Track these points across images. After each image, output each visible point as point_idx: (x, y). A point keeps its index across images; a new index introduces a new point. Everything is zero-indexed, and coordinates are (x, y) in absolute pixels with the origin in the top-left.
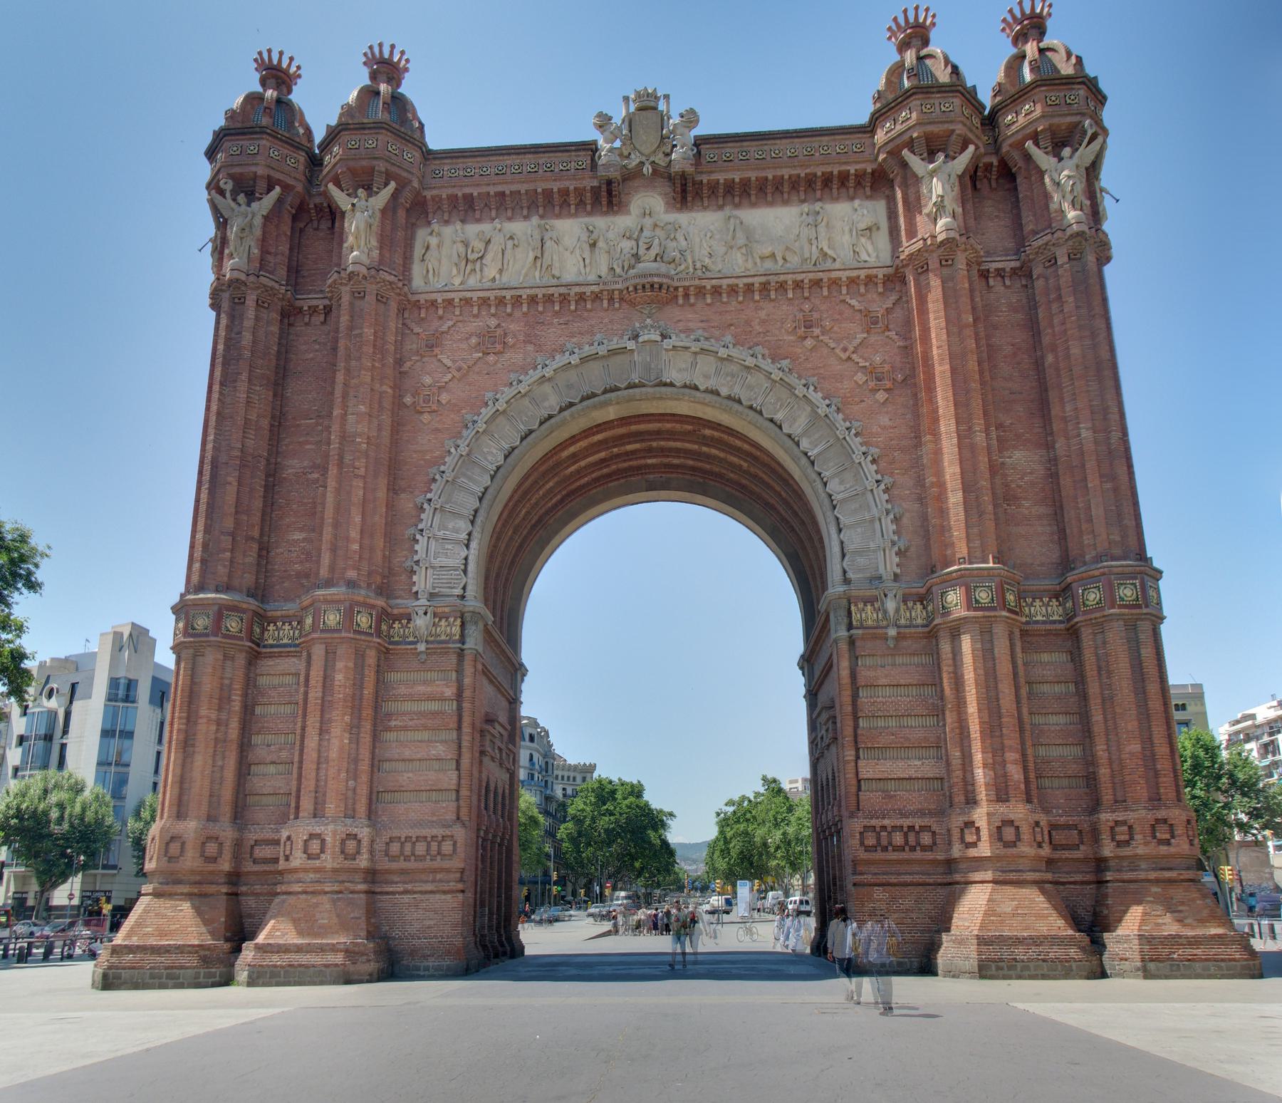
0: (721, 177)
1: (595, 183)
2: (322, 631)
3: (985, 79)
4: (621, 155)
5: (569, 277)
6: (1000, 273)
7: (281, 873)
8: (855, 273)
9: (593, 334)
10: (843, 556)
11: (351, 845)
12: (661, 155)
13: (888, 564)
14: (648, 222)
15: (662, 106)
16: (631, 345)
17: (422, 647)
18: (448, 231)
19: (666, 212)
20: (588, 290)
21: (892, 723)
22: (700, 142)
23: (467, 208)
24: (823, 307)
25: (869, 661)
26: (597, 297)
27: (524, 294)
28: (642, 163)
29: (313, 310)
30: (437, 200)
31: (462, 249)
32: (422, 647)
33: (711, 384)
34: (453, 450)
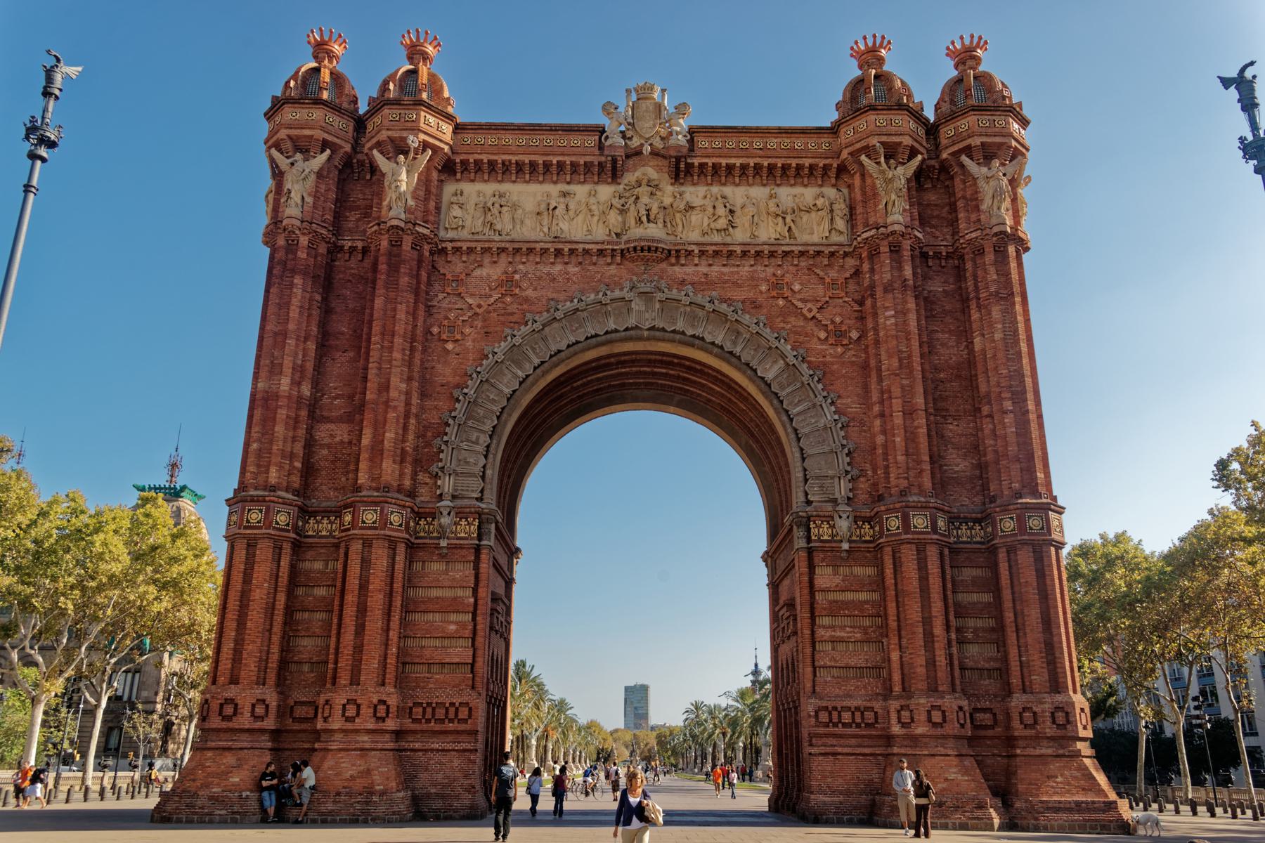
0: (710, 161)
1: (603, 159)
2: (362, 528)
3: (928, 98)
4: (624, 137)
6: (937, 255)
7: (317, 735)
10: (806, 481)
11: (382, 708)
12: (658, 139)
13: (842, 489)
16: (628, 296)
17: (443, 543)
22: (692, 131)
26: (601, 252)
28: (642, 145)
30: (464, 163)
33: (698, 332)
34: (475, 375)
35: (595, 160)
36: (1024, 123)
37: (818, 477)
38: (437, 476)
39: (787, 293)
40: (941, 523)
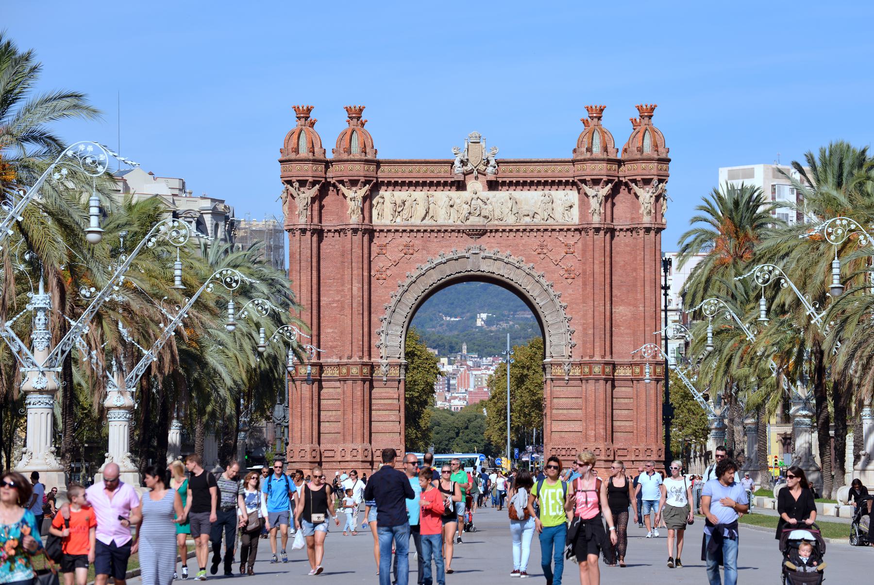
0: (508, 180)
5: (441, 221)
6: (621, 230)
8: (562, 227)
9: (451, 247)
13: (566, 351)
14: (475, 196)
16: (467, 255)
19: (483, 190)
20: (449, 229)
21: (565, 412)
22: (498, 163)
23: (395, 184)
24: (549, 240)
25: (558, 389)
26: (453, 231)
27: (422, 229)
29: (329, 231)
30: (383, 182)
33: (501, 273)
35: (449, 180)
37: (555, 345)
39: (545, 251)
40: (607, 370)
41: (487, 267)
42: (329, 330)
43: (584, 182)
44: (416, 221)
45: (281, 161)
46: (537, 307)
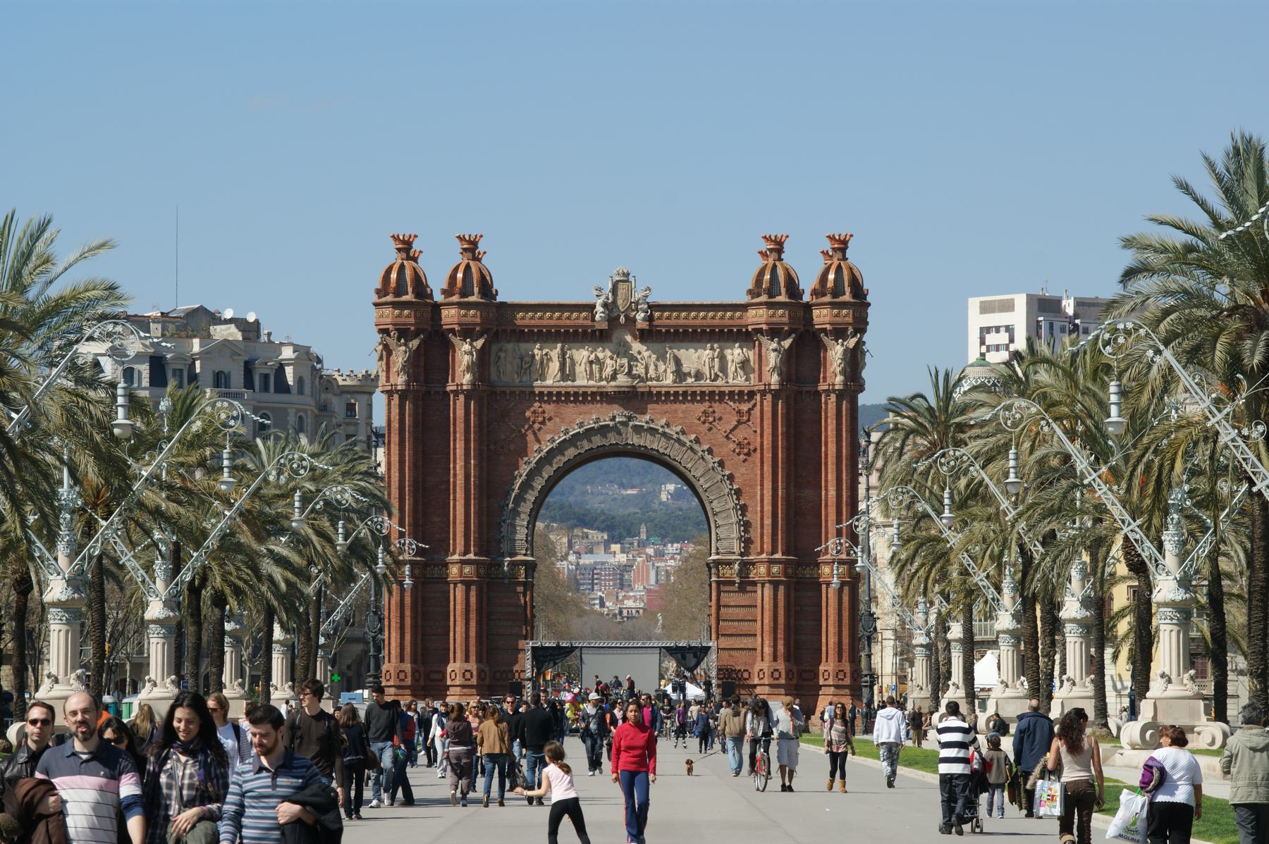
15: (631, 279)
16: (611, 423)
17: (506, 581)
18: (510, 346)
20: (589, 391)
22: (651, 307)
26: (593, 394)
30: (505, 331)
31: (518, 361)
32: (506, 581)
36: (869, 304)
38: (499, 542)
41: (635, 440)
42: (436, 519)
43: (760, 331)
44: (549, 382)
45: (376, 305)
46: (700, 490)
